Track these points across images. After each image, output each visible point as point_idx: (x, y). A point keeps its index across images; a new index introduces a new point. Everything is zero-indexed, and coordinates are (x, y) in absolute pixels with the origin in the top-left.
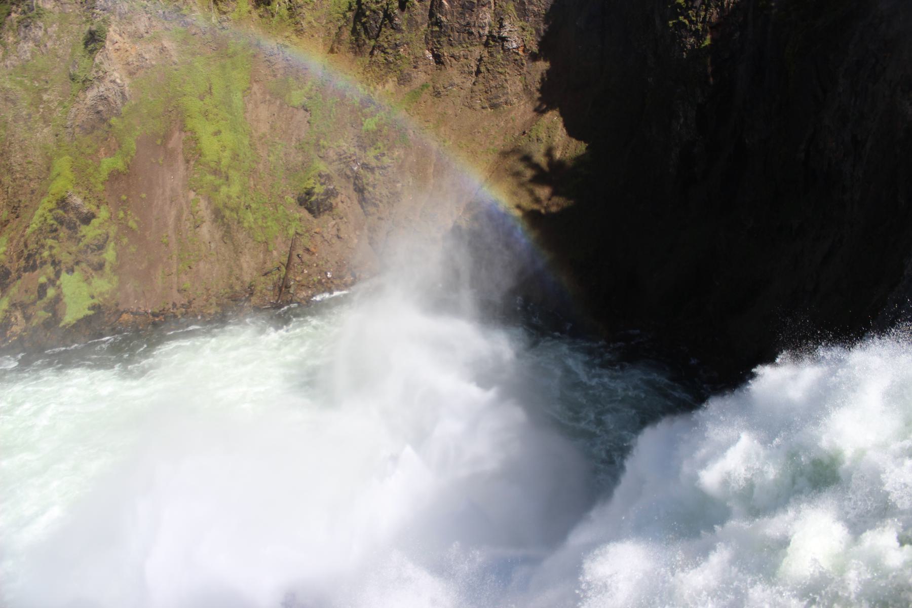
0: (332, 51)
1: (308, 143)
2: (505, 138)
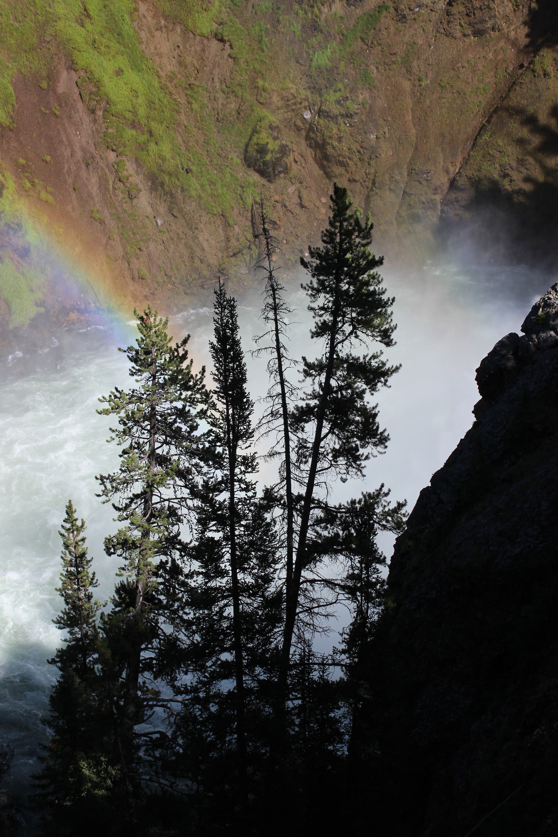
2: (495, 73)
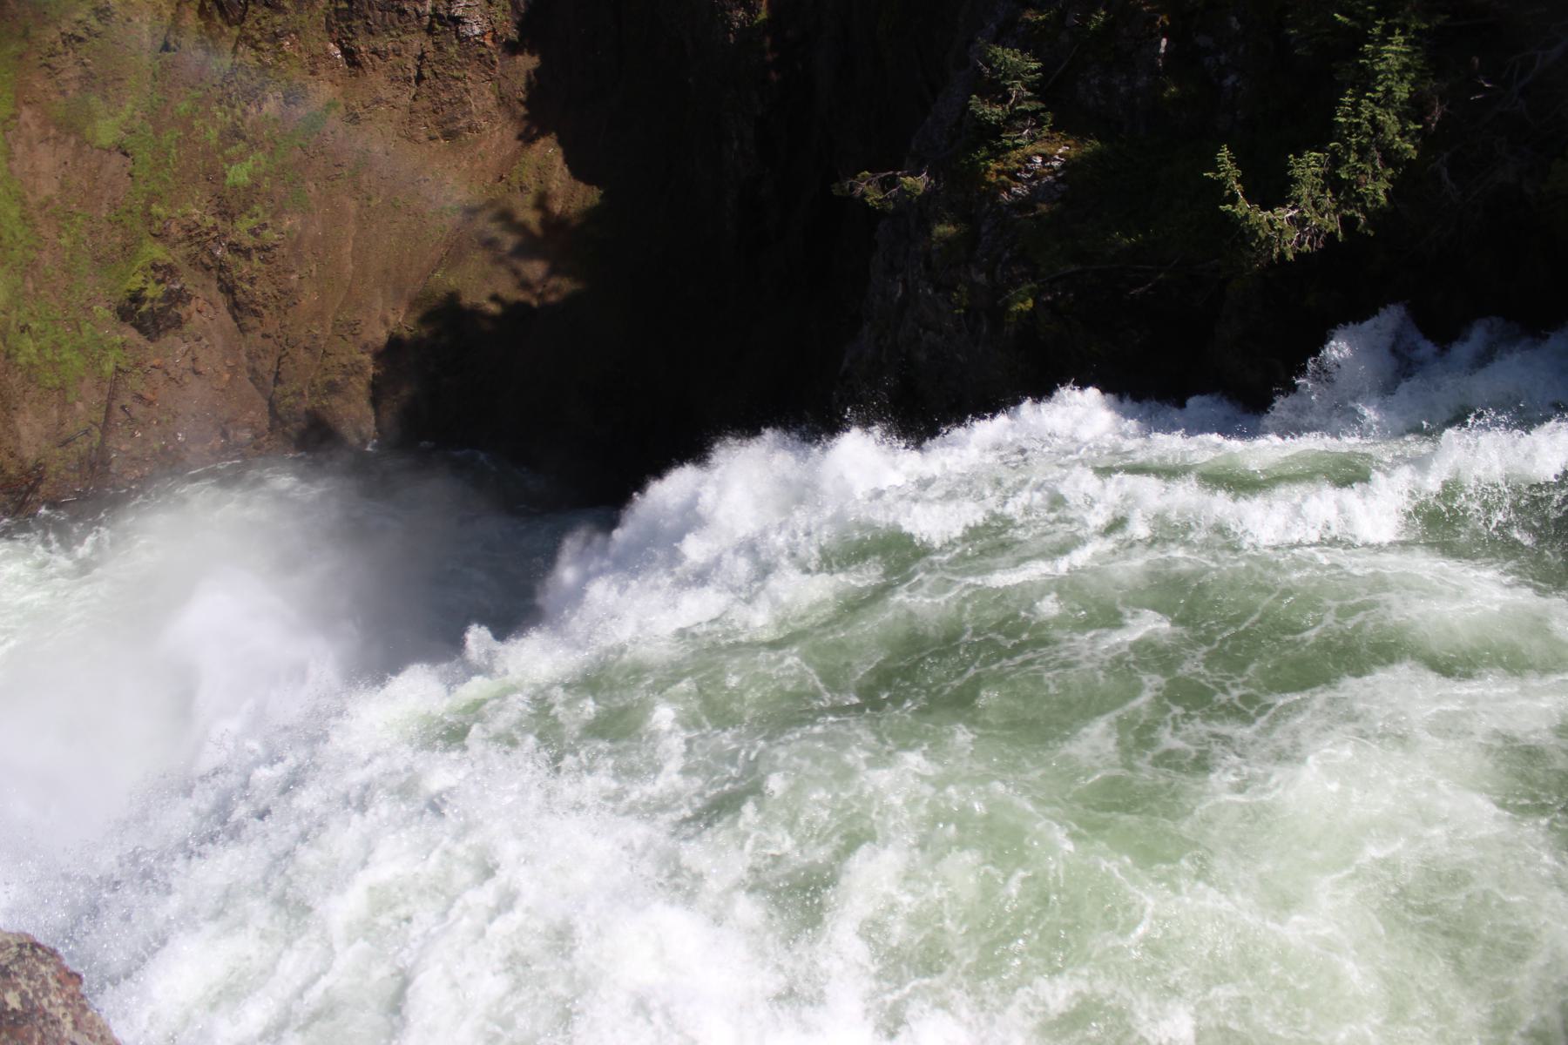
0: (166, 47)
1: (130, 212)
